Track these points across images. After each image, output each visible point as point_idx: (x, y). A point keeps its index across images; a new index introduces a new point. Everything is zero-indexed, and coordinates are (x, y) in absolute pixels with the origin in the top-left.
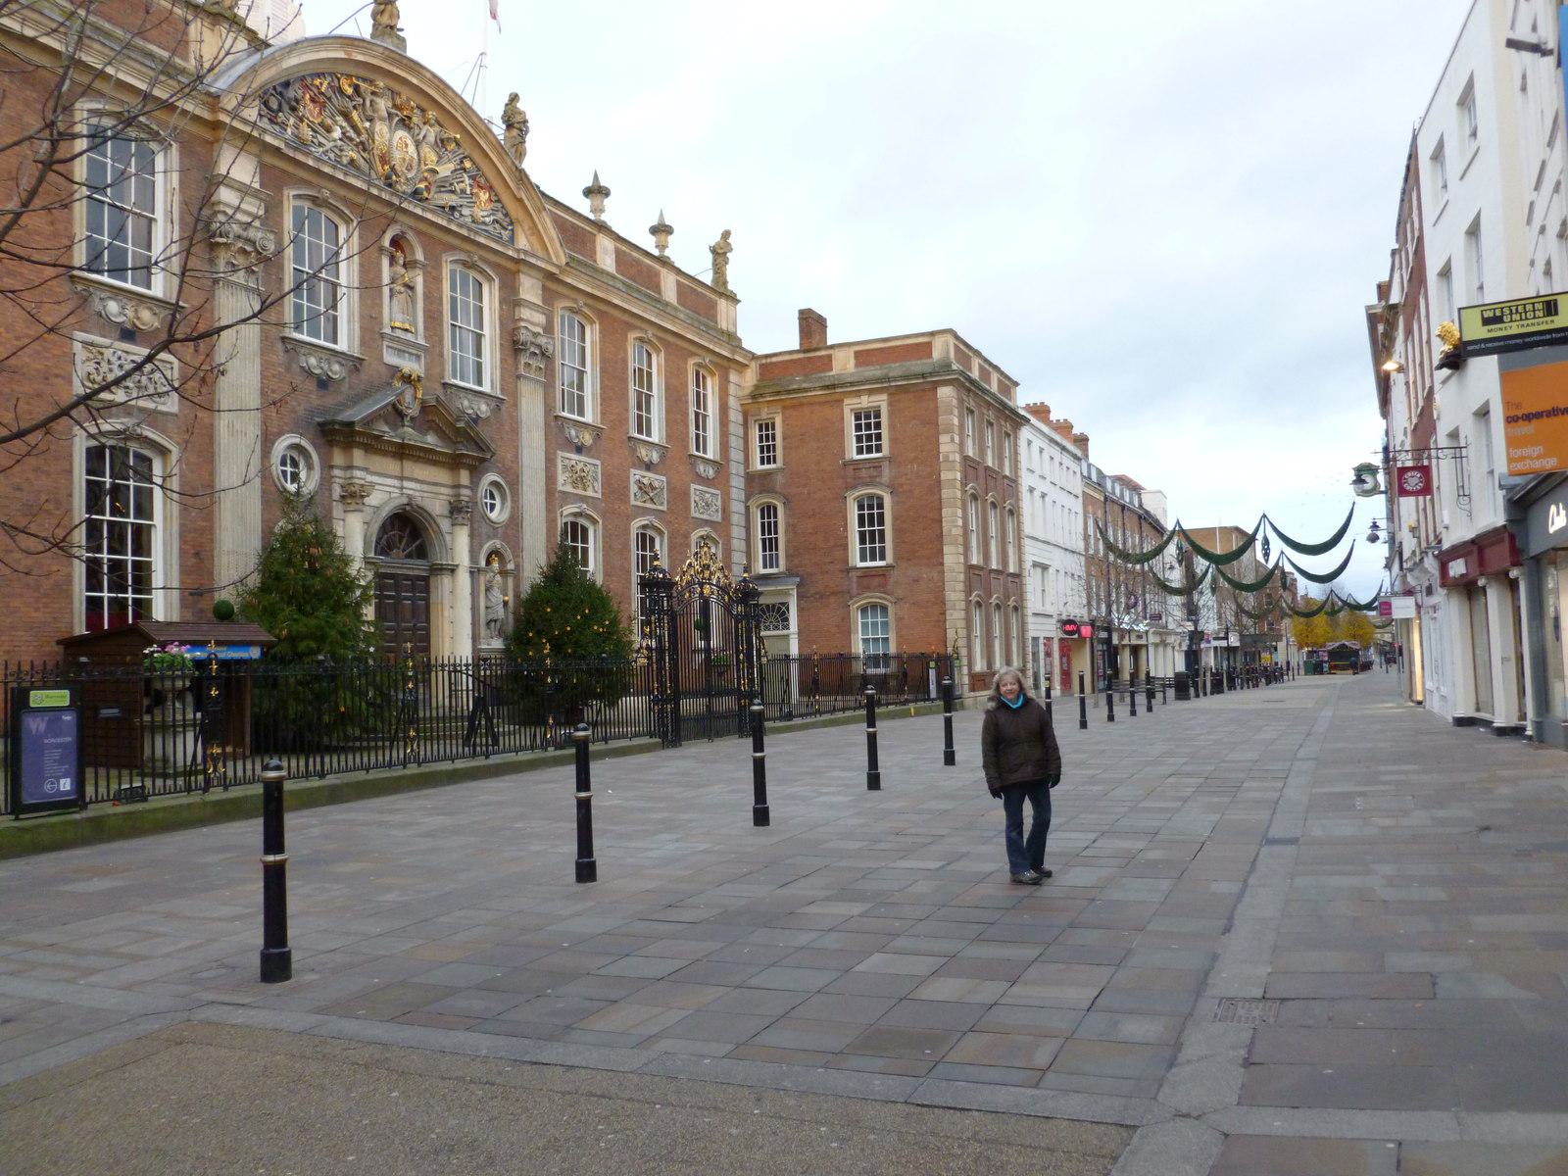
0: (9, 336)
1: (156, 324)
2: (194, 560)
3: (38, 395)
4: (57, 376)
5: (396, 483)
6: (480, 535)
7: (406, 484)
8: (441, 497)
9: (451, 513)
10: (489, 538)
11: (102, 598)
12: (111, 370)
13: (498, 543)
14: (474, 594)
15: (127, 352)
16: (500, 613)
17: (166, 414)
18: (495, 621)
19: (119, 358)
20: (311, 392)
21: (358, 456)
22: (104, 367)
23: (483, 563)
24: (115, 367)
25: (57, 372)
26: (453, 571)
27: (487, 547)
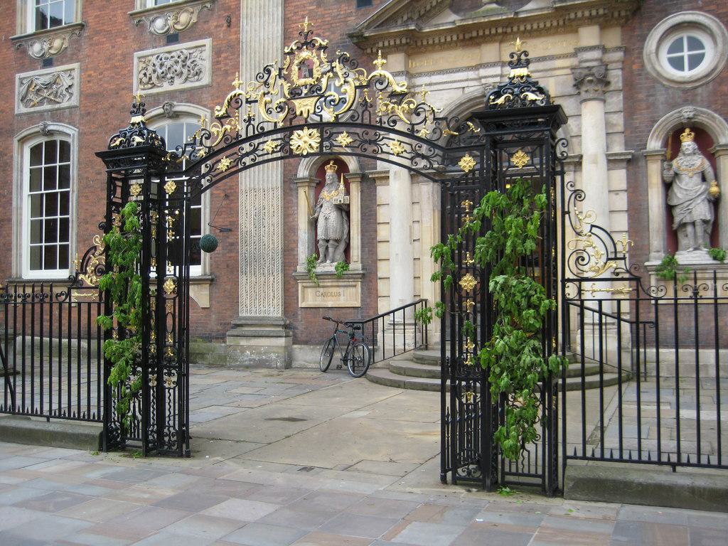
0: (95, 74)
1: (194, 20)
2: (225, 203)
3: (112, 107)
4: (123, 89)
5: (471, 74)
6: (651, 106)
7: (483, 72)
8: (558, 72)
9: (579, 84)
10: (674, 106)
11: (60, 246)
12: (154, 71)
13: (687, 112)
14: (636, 191)
15: (169, 52)
16: (702, 211)
17: (201, 88)
18: (693, 224)
19: (161, 59)
20: (350, 15)
21: (397, 61)
22: (150, 69)
23: (654, 144)
24: (157, 68)
25: (123, 86)
26: (580, 164)
27: (668, 119)
